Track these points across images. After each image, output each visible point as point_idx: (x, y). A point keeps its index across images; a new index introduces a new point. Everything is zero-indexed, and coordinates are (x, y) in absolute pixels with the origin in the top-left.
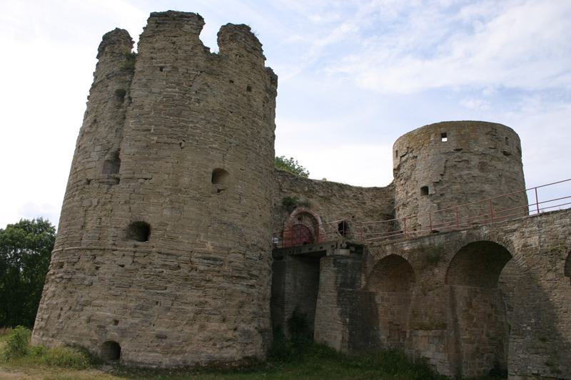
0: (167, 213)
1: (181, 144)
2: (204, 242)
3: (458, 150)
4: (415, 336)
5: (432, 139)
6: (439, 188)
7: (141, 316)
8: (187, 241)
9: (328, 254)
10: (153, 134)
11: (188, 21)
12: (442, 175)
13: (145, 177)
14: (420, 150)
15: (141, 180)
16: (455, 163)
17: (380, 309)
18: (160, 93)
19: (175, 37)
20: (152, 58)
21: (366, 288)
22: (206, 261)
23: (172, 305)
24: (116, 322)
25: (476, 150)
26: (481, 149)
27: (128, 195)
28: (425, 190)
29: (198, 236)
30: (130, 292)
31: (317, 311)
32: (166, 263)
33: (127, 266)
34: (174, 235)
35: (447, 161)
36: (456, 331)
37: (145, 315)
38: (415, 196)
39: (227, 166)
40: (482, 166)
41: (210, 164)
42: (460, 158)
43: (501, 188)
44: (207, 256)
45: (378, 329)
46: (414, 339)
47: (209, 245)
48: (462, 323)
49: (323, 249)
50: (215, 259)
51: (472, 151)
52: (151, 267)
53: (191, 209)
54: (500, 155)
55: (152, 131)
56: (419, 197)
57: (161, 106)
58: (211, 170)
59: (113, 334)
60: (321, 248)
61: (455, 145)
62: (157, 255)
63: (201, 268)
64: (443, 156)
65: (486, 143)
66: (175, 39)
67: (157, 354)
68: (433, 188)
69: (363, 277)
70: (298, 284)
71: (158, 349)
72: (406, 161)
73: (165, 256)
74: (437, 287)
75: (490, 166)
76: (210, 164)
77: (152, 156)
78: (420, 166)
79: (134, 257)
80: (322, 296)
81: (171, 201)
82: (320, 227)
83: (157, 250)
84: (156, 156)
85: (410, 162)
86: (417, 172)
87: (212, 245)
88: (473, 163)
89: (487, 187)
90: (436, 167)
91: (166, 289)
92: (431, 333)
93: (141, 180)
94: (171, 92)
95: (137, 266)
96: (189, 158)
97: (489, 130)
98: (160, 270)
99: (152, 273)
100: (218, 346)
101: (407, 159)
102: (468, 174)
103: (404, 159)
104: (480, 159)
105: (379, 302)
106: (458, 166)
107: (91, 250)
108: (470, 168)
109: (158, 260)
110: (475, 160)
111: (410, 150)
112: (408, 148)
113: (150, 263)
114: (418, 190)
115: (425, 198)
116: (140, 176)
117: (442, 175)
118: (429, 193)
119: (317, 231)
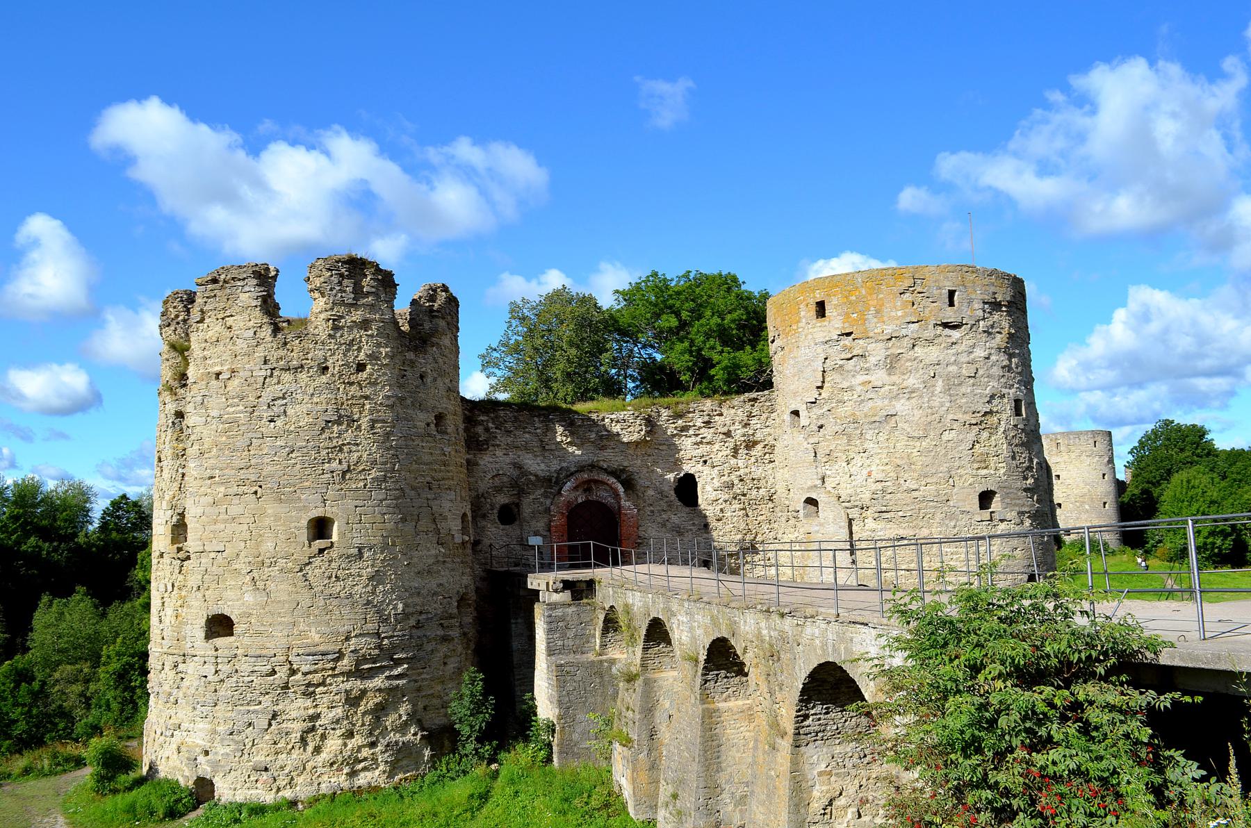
0: (249, 598)
1: (256, 493)
5: (802, 313)
6: (816, 411)
8: (280, 634)
15: (213, 555)
16: (841, 362)
18: (220, 417)
19: (232, 316)
22: (311, 657)
23: (270, 725)
24: (207, 753)
25: (879, 330)
26: (889, 329)
27: (200, 577)
32: (256, 668)
33: (210, 678)
34: (263, 628)
35: (826, 359)
39: (329, 511)
40: (892, 363)
43: (936, 404)
44: (313, 650)
47: (313, 634)
51: (871, 334)
53: (282, 586)
57: (224, 438)
59: (205, 770)
61: (840, 325)
63: (305, 668)
64: (820, 349)
65: (900, 313)
73: (253, 659)
82: (623, 502)
88: (872, 360)
89: (901, 406)
93: (213, 555)
95: (221, 677)
98: (250, 679)
102: (864, 384)
106: (846, 368)
108: (868, 369)
109: (244, 666)
110: (877, 352)
117: (818, 387)
119: (620, 507)
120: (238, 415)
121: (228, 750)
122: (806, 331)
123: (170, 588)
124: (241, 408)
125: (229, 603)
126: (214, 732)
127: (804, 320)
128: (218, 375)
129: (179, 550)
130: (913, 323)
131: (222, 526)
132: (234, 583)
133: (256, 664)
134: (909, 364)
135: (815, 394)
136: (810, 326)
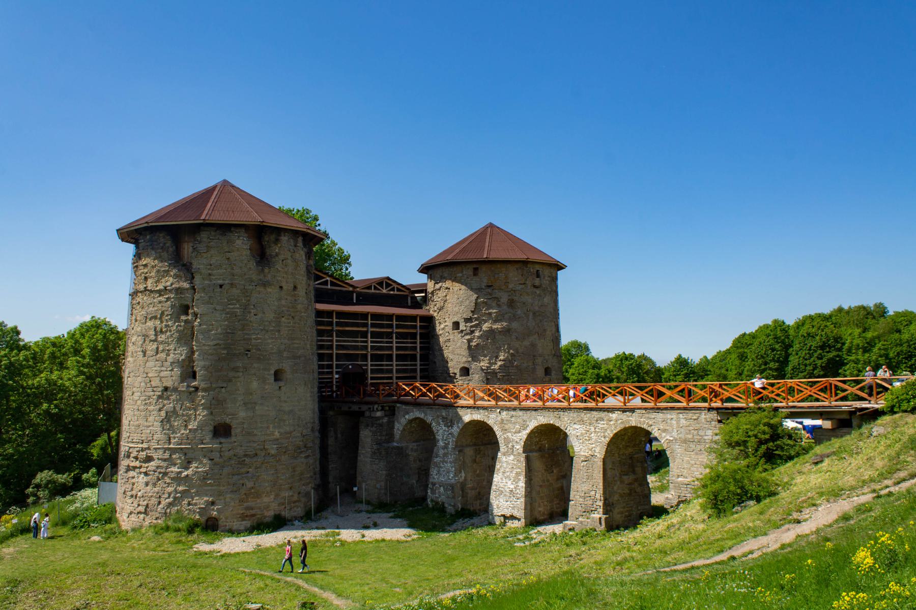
3: (489, 286)
8: (260, 434)
11: (239, 237)
13: (221, 385)
17: (411, 459)
20: (210, 275)
28: (456, 325)
29: (268, 428)
32: (247, 453)
42: (490, 294)
52: (235, 458)
56: (451, 332)
58: (272, 372)
66: (228, 255)
68: (464, 324)
70: (339, 435)
72: (439, 289)
80: (361, 451)
86: (450, 305)
87: (279, 432)
88: (502, 300)
98: (244, 459)
101: (441, 287)
104: (509, 296)
118: (461, 329)
124: (238, 306)
128: (221, 286)
134: (518, 304)
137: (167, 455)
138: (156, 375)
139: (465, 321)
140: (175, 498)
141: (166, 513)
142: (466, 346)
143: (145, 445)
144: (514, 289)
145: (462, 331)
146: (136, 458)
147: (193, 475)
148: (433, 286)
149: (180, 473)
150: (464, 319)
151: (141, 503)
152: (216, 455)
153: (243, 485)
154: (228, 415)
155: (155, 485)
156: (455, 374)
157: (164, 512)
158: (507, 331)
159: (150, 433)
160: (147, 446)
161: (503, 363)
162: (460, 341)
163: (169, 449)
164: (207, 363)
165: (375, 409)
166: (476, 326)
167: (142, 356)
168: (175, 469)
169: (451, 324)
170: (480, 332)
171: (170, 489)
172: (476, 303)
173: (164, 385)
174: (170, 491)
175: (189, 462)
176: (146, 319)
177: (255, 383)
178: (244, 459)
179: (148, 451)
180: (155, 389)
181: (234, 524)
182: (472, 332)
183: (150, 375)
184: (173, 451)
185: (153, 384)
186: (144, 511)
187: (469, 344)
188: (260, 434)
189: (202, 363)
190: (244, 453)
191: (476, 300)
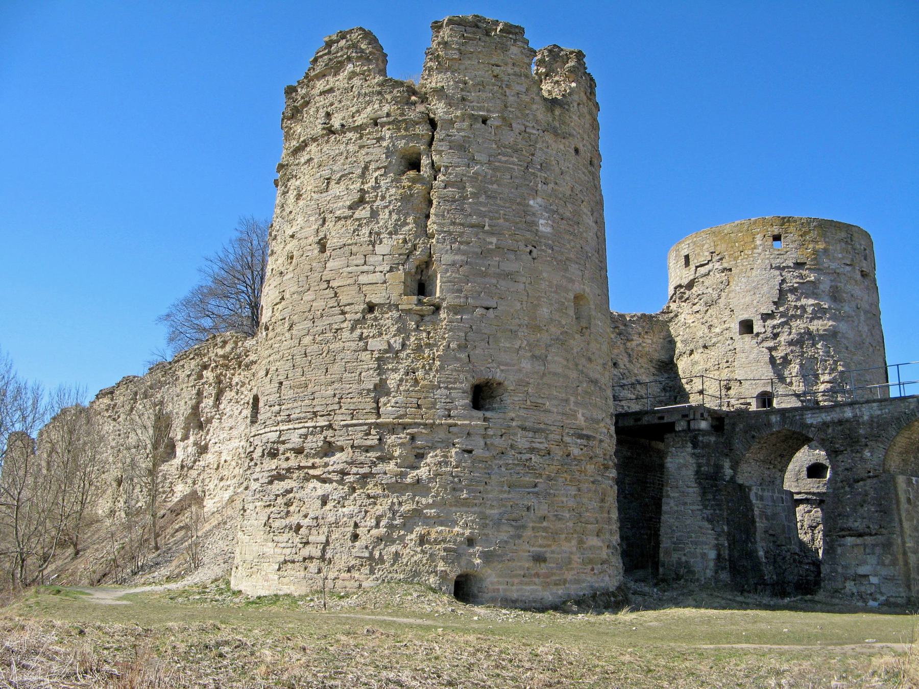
0: (526, 365)
1: (531, 252)
2: (575, 411)
4: (840, 546)
5: (758, 242)
6: (770, 323)
7: (510, 529)
8: (555, 410)
9: (678, 428)
10: (487, 232)
11: (515, 41)
12: (775, 303)
14: (736, 259)
17: (757, 512)
21: (733, 479)
22: (579, 441)
25: (826, 265)
26: (833, 266)
28: (747, 327)
29: (567, 401)
30: (487, 492)
31: (664, 517)
34: (540, 401)
36: (902, 536)
37: (517, 528)
38: (727, 334)
41: (570, 286)
45: (756, 542)
46: (839, 550)
48: (906, 525)
49: (665, 421)
50: (588, 437)
53: (556, 358)
54: (858, 276)
55: (487, 228)
56: (737, 337)
60: (662, 418)
62: (520, 433)
64: (778, 272)
65: (840, 256)
66: (497, 70)
67: (535, 587)
69: (727, 464)
71: (536, 580)
73: (531, 434)
74: (869, 477)
75: (844, 292)
76: (570, 286)
77: (492, 270)
78: (739, 285)
79: (485, 436)
81: (529, 344)
83: (519, 423)
84: (498, 270)
85: (718, 277)
87: (583, 415)
88: (821, 287)
90: (766, 288)
91: (536, 486)
92: (868, 540)
94: (506, 162)
96: (545, 275)
97: (843, 235)
99: (516, 462)
100: (595, 571)
103: (702, 270)
104: (831, 281)
105: (754, 502)
107: (405, 427)
109: (522, 441)
111: (716, 258)
112: (712, 253)
113: (512, 446)
114: (735, 327)
115: (747, 337)
116: (478, 303)
118: (755, 331)
120: (511, 166)
121: (504, 536)
122: (762, 256)
123: (397, 346)
125: (502, 367)
126: (483, 516)
127: (761, 248)
129: (420, 302)
130: (848, 265)
131: (494, 281)
132: (508, 345)
133: (534, 440)
134: (845, 295)
135: (774, 308)
136: (767, 253)
137: (373, 441)
138: (351, 281)
139: (762, 318)
140: (391, 527)
141: (371, 558)
142: (767, 358)
143: (322, 422)
144: (838, 271)
145: (758, 334)
146: (299, 451)
147: (430, 480)
148: (693, 272)
149: (403, 475)
150: (763, 314)
151: (311, 539)
152: (477, 444)
153: (528, 509)
154: (500, 364)
155: (341, 502)
156: (749, 404)
157: (367, 555)
158: (831, 336)
159: (335, 395)
160: (327, 423)
161: (829, 386)
162: (756, 351)
163: (377, 425)
164: (458, 258)
165: (698, 416)
166: (782, 325)
167: (316, 252)
168: (391, 466)
169: (738, 326)
170: (790, 333)
171: (379, 509)
172: (781, 290)
173: (367, 300)
174: (378, 513)
175: (420, 456)
176: (328, 183)
177: (545, 310)
178: (528, 456)
179: (330, 433)
180: (347, 309)
181: (514, 588)
182: (776, 336)
183: (334, 284)
184: (393, 429)
185: (344, 299)
186: (319, 554)
187: (771, 355)
188: (555, 410)
189: (447, 258)
190: (527, 445)
191: (781, 284)
